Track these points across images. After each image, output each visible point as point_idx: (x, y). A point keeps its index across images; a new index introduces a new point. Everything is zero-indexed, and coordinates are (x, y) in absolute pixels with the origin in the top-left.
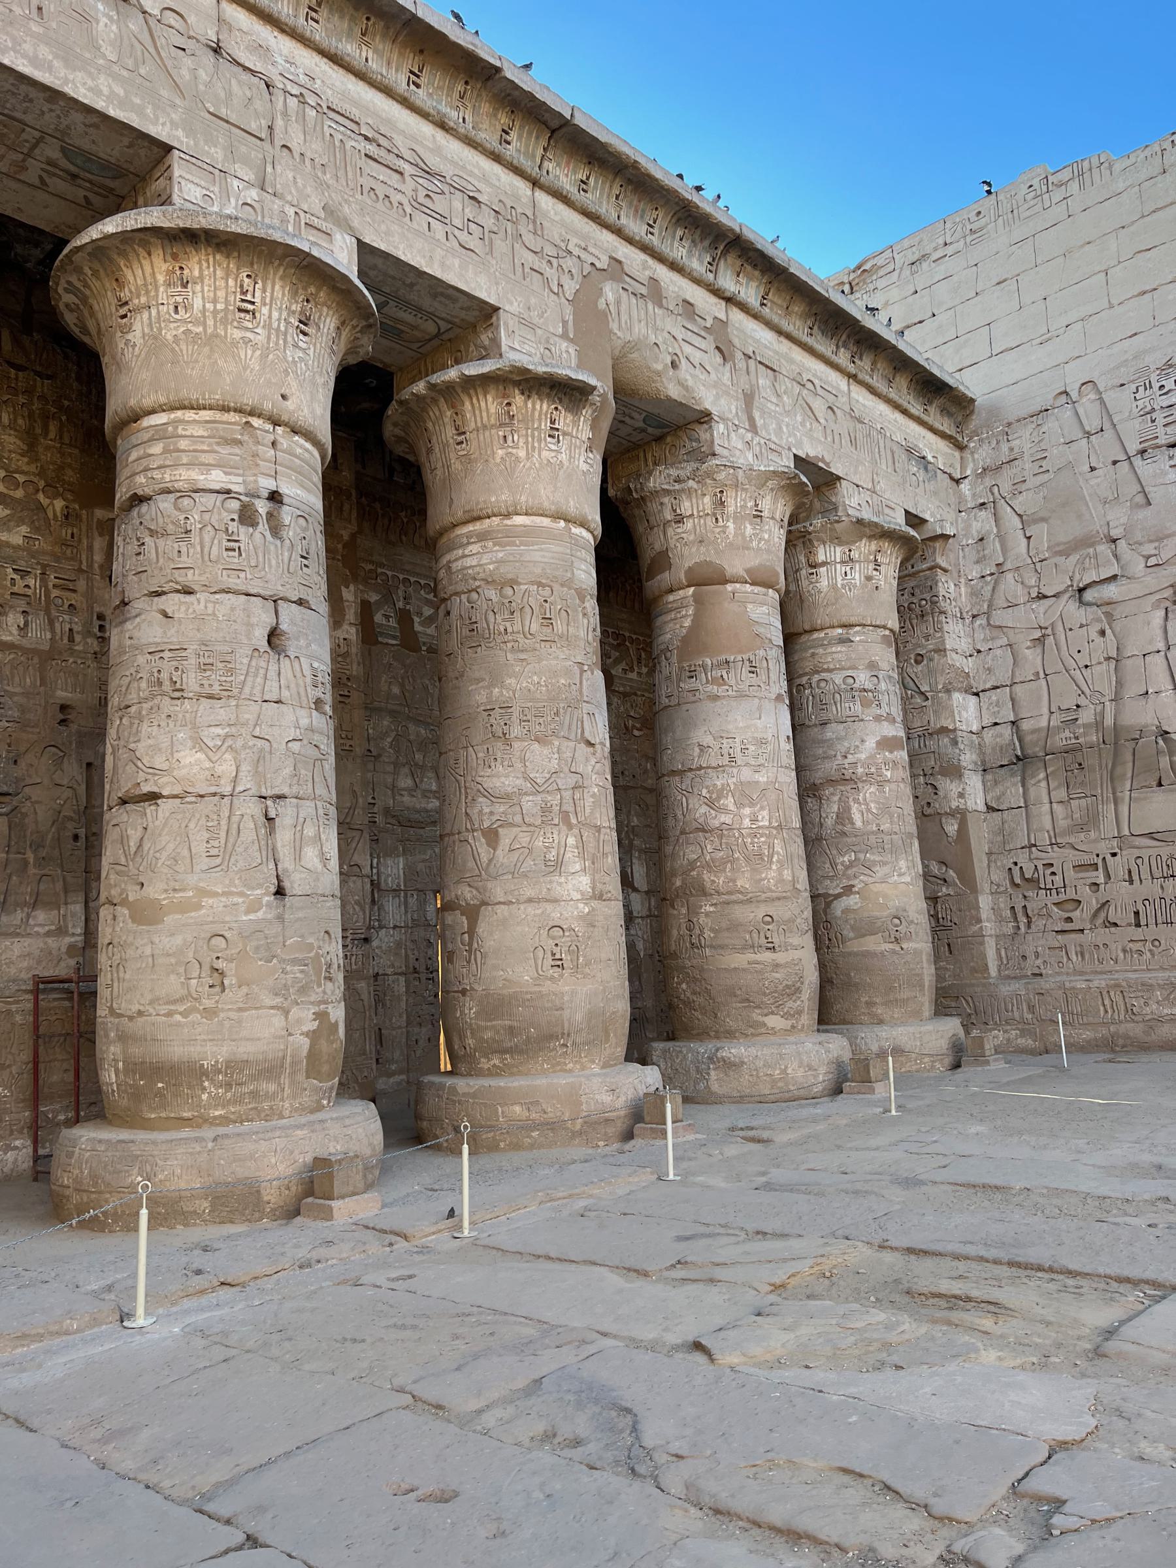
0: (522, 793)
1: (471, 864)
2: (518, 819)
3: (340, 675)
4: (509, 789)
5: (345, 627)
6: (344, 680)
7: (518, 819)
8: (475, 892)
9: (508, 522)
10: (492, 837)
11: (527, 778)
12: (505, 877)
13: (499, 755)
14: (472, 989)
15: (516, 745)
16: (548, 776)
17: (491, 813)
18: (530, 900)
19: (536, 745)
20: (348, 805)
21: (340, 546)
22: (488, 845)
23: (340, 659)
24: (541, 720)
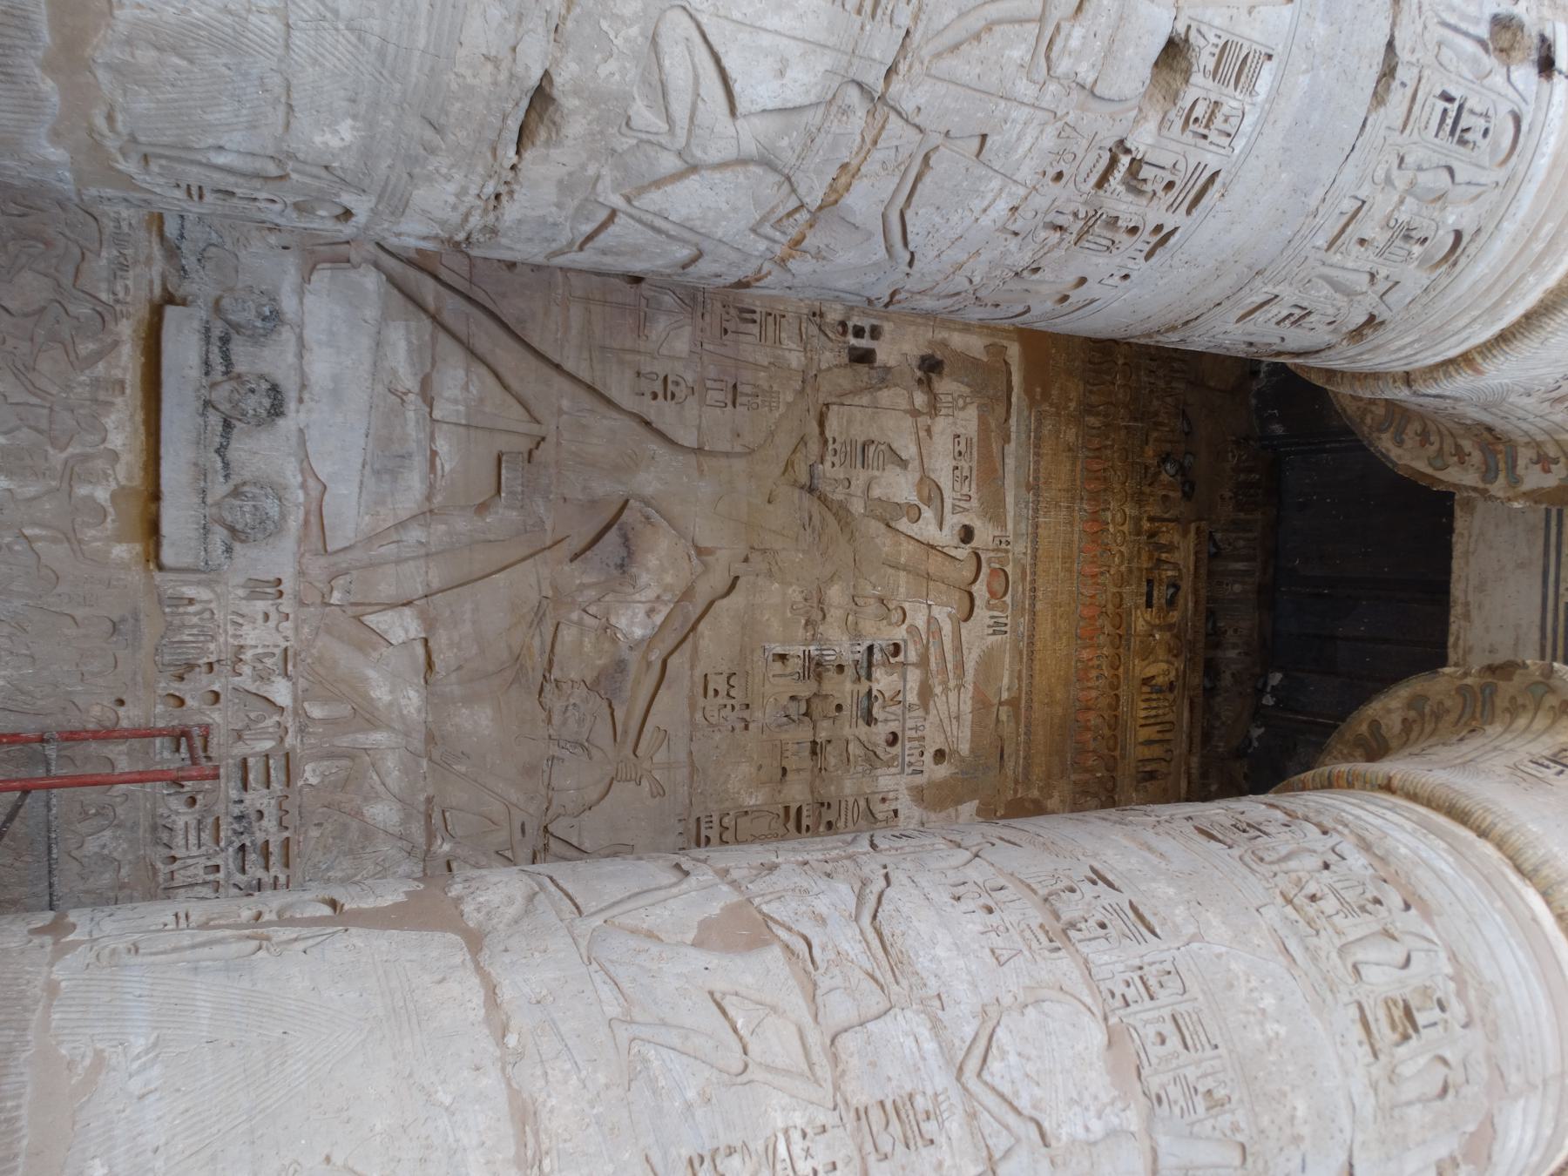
0: (934, 1008)
1: (614, 890)
2: (839, 1009)
3: (835, 806)
4: (923, 963)
5: (917, 812)
6: (830, 815)
7: (839, 1009)
8: (512, 911)
9: (1514, 878)
10: (745, 931)
11: (990, 1017)
12: (606, 992)
13: (1010, 916)
14: (60, 951)
15: (1064, 966)
16: (1024, 1103)
17: (821, 920)
18: (524, 1115)
19: (1099, 1037)
20: (587, 846)
21: (1035, 793)
22: (705, 925)
23: (862, 803)
24: (1174, 1042)
